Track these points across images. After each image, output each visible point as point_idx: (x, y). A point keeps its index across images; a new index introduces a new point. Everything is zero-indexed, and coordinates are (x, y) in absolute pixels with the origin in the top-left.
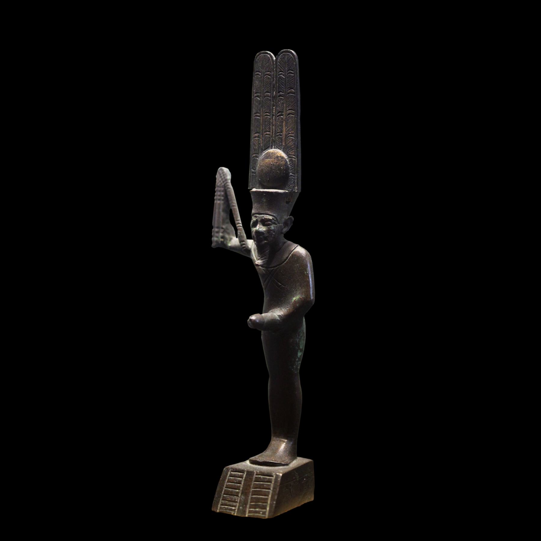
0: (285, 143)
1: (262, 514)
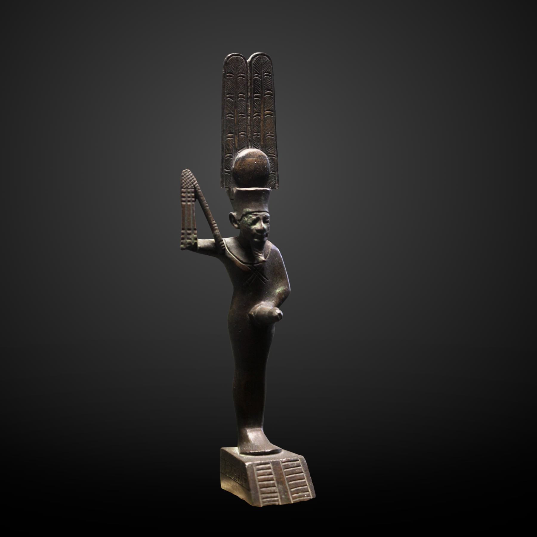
1: (307, 496)
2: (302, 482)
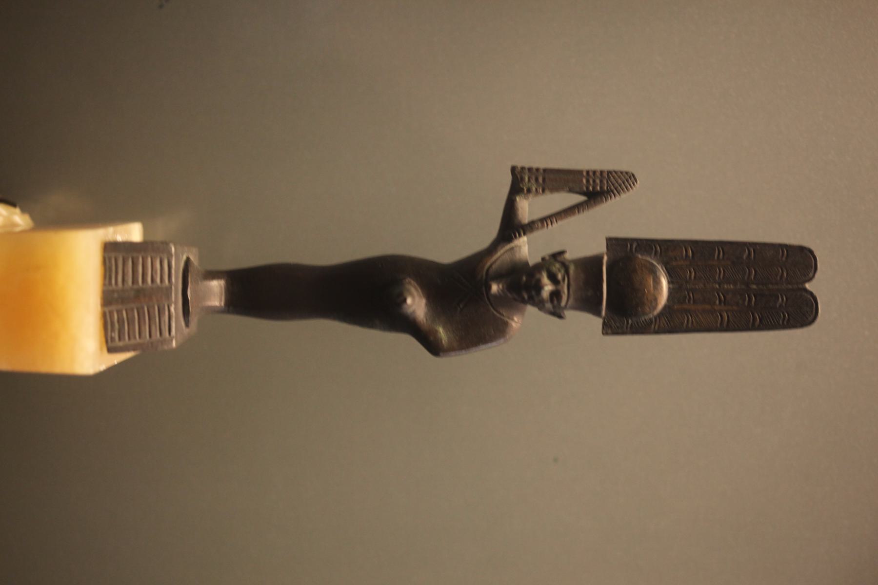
2: (134, 332)
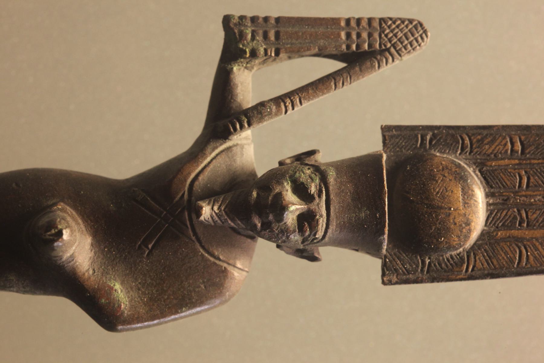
0: (503, 240)
